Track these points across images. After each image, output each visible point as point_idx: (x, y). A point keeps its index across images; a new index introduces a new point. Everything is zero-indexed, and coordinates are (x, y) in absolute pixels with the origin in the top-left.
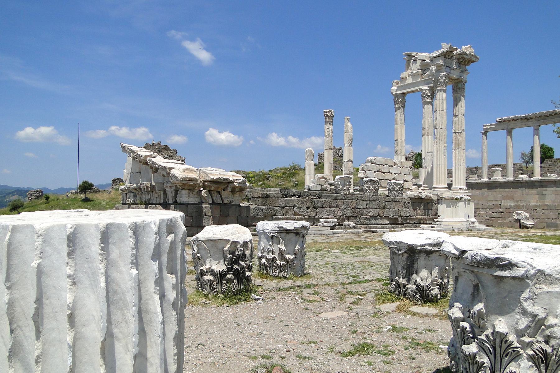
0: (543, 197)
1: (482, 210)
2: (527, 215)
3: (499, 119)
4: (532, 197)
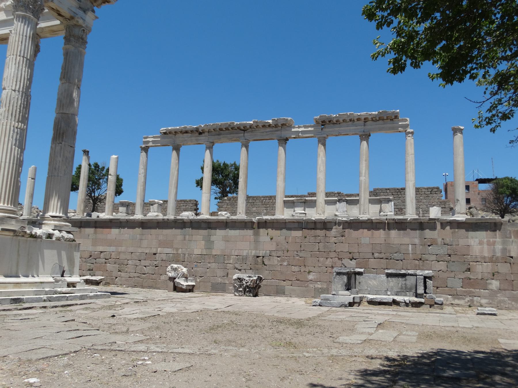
0: (209, 244)
1: (130, 262)
2: (185, 270)
3: (163, 129)
4: (197, 243)
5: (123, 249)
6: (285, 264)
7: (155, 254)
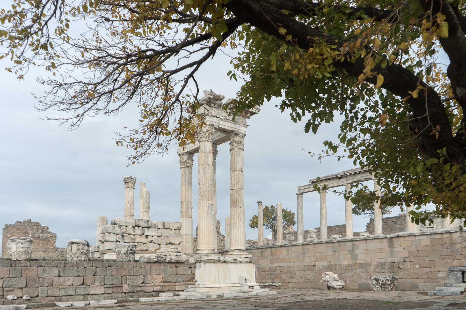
1: (297, 272)
5: (291, 264)
6: (417, 266)
7: (314, 266)
